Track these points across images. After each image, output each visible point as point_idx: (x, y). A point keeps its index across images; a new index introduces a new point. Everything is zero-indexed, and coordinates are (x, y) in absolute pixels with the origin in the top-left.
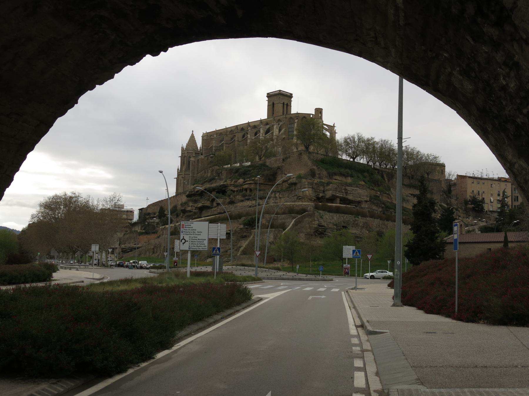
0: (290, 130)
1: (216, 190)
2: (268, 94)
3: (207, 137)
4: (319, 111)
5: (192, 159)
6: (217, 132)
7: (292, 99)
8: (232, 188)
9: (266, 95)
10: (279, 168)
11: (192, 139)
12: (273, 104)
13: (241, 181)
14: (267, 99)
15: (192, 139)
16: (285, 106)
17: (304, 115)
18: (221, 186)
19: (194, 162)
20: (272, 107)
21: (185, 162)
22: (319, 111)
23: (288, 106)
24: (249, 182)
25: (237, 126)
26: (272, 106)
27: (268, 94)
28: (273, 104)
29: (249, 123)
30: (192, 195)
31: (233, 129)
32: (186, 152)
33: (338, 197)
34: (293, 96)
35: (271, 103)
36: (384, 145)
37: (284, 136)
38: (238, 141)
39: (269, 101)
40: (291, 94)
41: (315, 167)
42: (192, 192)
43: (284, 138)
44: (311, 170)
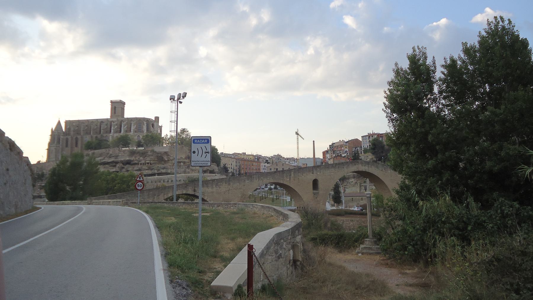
2: (111, 101)
3: (67, 123)
4: (157, 118)
5: (62, 137)
9: (110, 101)
11: (59, 123)
12: (115, 108)
13: (141, 158)
14: (110, 104)
15: (59, 123)
22: (157, 118)
23: (123, 109)
24: (149, 159)
25: (97, 119)
27: (111, 101)
28: (115, 108)
31: (93, 120)
33: (208, 170)
34: (126, 103)
35: (113, 107)
37: (136, 130)
38: (103, 129)
39: (111, 105)
40: (125, 103)
44: (188, 155)
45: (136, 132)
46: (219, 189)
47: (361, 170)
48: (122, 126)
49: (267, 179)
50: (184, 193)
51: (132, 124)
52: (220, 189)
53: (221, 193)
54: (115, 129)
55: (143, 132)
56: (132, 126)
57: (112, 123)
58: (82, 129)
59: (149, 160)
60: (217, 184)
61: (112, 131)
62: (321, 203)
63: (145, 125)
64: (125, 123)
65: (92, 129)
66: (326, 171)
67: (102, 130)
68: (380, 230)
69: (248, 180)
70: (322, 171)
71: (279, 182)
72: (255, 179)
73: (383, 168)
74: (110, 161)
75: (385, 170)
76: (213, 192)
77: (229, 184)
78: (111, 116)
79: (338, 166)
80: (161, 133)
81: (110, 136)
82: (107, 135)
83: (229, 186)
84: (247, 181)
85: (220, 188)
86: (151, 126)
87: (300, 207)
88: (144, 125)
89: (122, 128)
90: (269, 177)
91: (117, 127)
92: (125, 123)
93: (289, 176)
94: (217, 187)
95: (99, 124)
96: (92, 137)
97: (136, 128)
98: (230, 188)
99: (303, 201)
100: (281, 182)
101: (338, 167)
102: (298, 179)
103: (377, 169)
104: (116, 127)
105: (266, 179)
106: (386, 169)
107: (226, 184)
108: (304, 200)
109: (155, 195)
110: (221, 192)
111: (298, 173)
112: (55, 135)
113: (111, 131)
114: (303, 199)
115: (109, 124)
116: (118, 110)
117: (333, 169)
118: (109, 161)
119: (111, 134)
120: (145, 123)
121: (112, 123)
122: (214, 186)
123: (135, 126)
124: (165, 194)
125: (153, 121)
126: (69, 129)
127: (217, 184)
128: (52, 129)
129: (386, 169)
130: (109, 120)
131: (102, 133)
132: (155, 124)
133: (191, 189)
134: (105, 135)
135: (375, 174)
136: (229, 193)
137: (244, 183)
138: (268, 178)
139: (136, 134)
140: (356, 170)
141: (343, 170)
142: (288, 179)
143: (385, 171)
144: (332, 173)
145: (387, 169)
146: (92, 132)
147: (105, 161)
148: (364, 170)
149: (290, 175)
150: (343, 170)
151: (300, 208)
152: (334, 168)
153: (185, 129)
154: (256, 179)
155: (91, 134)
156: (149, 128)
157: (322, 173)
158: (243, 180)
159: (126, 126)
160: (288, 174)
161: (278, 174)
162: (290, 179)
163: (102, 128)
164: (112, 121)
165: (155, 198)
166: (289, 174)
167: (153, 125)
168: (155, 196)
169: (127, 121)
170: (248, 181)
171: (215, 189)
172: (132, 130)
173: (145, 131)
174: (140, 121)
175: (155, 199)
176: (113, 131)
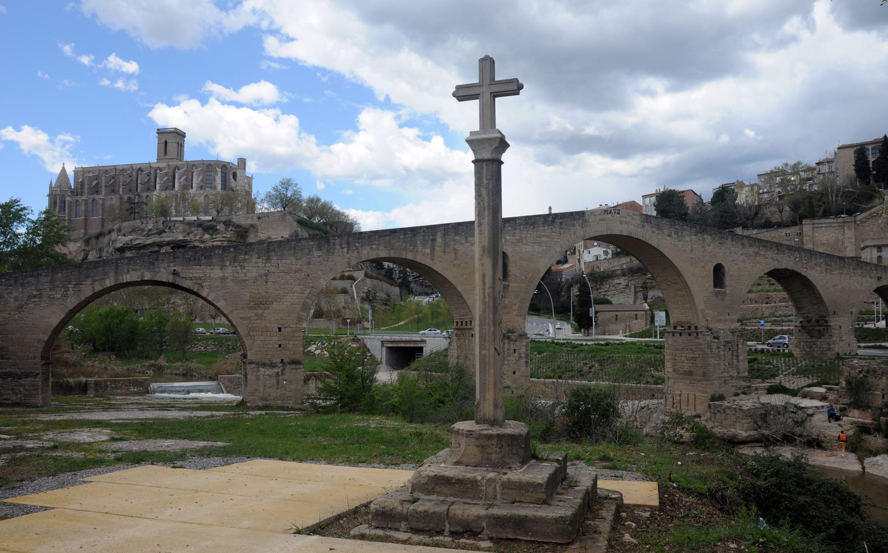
0: (208, 178)
1: (172, 245)
4: (242, 162)
5: (68, 199)
6: (100, 168)
7: (185, 139)
8: (196, 244)
10: (252, 226)
12: (166, 143)
13: (207, 236)
14: (157, 135)
16: (180, 146)
17: (224, 164)
18: (179, 241)
19: (71, 202)
20: (164, 147)
21: (58, 202)
22: (242, 162)
23: (181, 146)
24: (221, 239)
26: (163, 145)
27: (158, 130)
28: (166, 143)
29: (149, 163)
30: (127, 247)
32: (59, 189)
35: (163, 141)
36: (285, 199)
37: (202, 184)
38: (141, 184)
39: (159, 138)
40: (185, 133)
41: (299, 229)
42: (128, 244)
43: (201, 187)
45: (201, 188)
46: (240, 271)
47: (618, 233)
48: (177, 176)
49: (371, 248)
50: (146, 279)
51: (195, 173)
52: (244, 271)
53: (245, 280)
54: (164, 183)
55: (215, 188)
56: (194, 176)
57: (158, 171)
58: (103, 184)
59: (221, 241)
60: (235, 257)
61: (158, 186)
62: (515, 310)
63: (219, 174)
64: (182, 171)
65: (121, 184)
66: (528, 231)
67: (139, 186)
68: (338, 355)
69: (319, 247)
70: (517, 231)
71: (404, 257)
72: (338, 247)
73: (673, 229)
74: (149, 241)
75: (677, 234)
76: (223, 278)
77: (268, 259)
78: (159, 159)
79: (561, 220)
80: (249, 190)
81: (154, 196)
82: (148, 194)
83: (267, 265)
84: (316, 253)
85: (243, 267)
86: (231, 177)
87: (462, 322)
88: (217, 175)
89: (176, 180)
90: (377, 243)
91: (167, 180)
92: (182, 171)
93: (430, 242)
94: (237, 264)
95: (134, 174)
96: (121, 198)
97: (202, 181)
98: (272, 269)
99: (467, 305)
100: (410, 256)
101: (561, 223)
102: (455, 249)
103: (656, 232)
104: (165, 179)
105: (368, 248)
106: (680, 234)
107: (259, 258)
108: (468, 302)
109: (70, 282)
110: (247, 278)
111: (456, 235)
112: (55, 195)
113: (155, 188)
114: (465, 302)
115: (152, 172)
116: (172, 147)
117: (546, 228)
118: (147, 243)
119: (155, 193)
120: (219, 170)
121: (158, 171)
122: (228, 263)
123: (201, 177)
124: (95, 281)
125: (235, 167)
126: (82, 183)
127: (235, 257)
128: (51, 183)
129: (680, 234)
130: (153, 166)
131: (139, 190)
132: (239, 173)
133: (165, 269)
134: (144, 195)
135: (652, 244)
136: (267, 282)
137: (309, 257)
138: (373, 246)
139: (202, 192)
140: (606, 234)
141: (572, 232)
142: (428, 251)
143: (676, 236)
144: (544, 239)
145: (682, 233)
146: (121, 189)
147: (140, 244)
148: (625, 233)
149: (434, 240)
150: (572, 232)
151: (462, 325)
152: (548, 225)
153: (289, 180)
154: (342, 248)
155: (121, 193)
156: (227, 181)
157: (518, 238)
158: (306, 251)
159: (185, 177)
160: (427, 238)
161: (402, 237)
162: (433, 249)
163: (139, 182)
164: (159, 167)
165: (71, 289)
166: (431, 237)
167: (235, 176)
168: (71, 284)
169: (185, 168)
170: (319, 253)
171: (229, 271)
172: (194, 185)
173: (219, 187)
174: (210, 167)
175: (68, 293)
176: (160, 187)
